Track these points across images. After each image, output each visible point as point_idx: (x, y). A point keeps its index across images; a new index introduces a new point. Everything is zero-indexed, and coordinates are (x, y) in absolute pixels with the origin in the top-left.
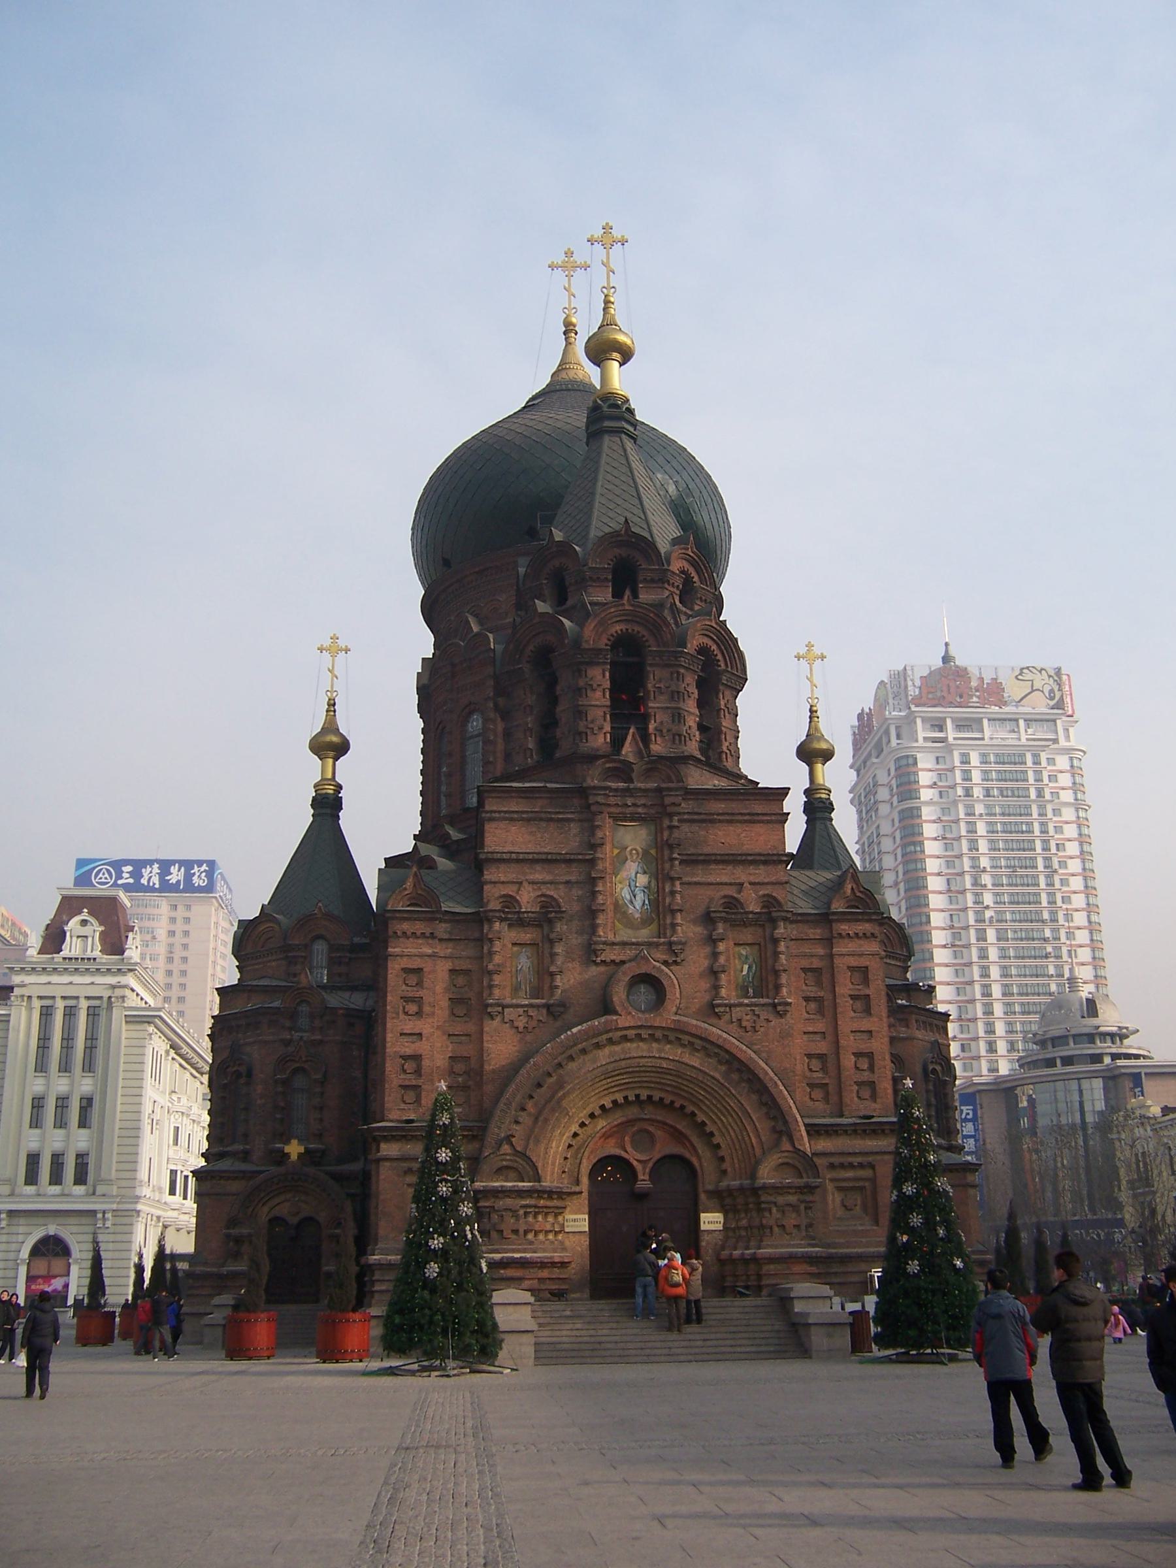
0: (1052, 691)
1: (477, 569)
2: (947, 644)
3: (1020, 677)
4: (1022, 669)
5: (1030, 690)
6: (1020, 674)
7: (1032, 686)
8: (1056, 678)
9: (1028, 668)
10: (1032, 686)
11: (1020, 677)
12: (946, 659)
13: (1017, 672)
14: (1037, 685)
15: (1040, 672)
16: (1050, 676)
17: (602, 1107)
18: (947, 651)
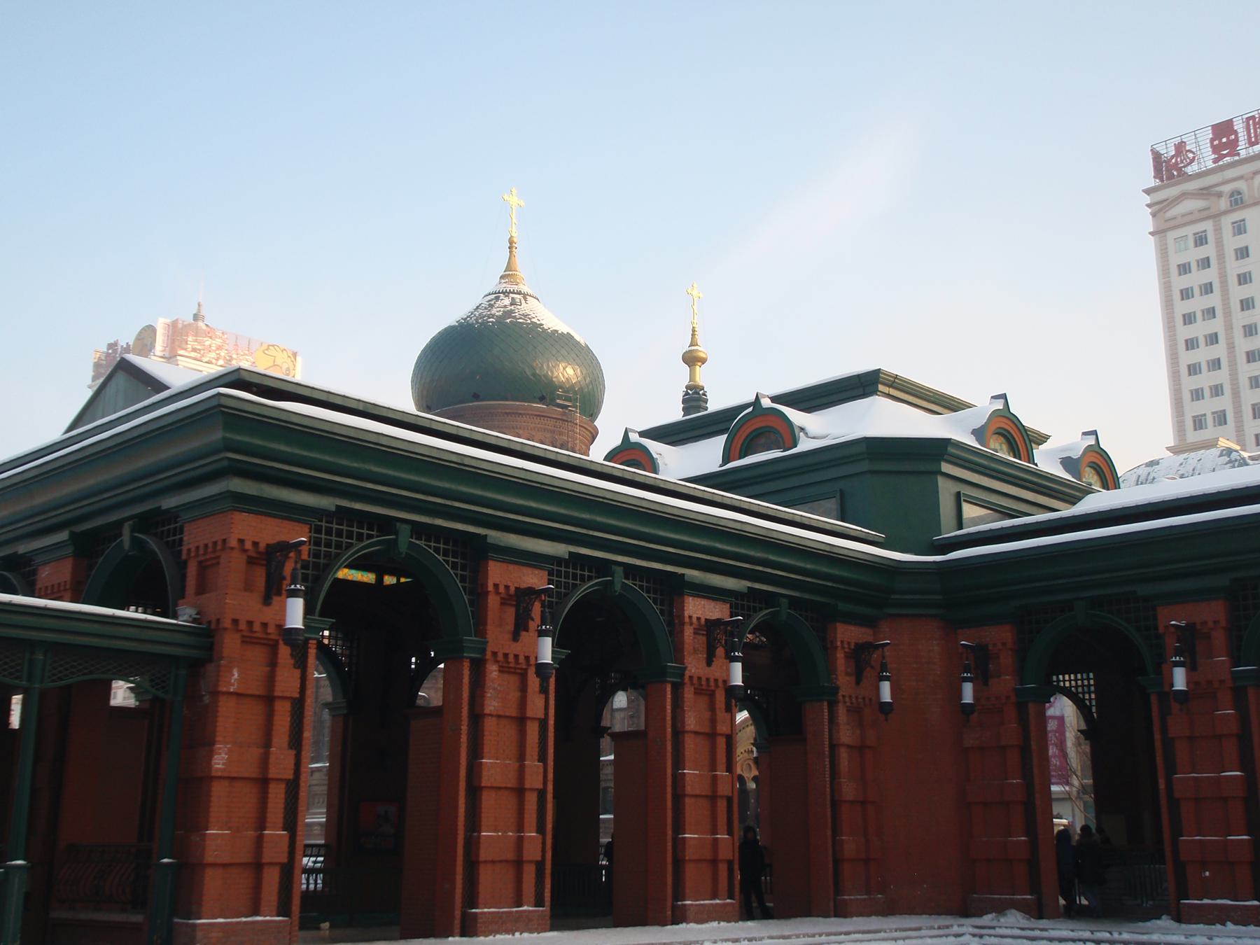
0: (288, 369)
1: (508, 411)
2: (199, 305)
3: (266, 352)
4: (269, 345)
5: (272, 364)
6: (267, 350)
7: (274, 362)
8: (293, 359)
9: (273, 346)
10: (274, 362)
11: (266, 352)
12: (196, 317)
13: (265, 347)
14: (278, 362)
15: (282, 351)
16: (289, 357)
17: (742, 753)
18: (199, 310)
